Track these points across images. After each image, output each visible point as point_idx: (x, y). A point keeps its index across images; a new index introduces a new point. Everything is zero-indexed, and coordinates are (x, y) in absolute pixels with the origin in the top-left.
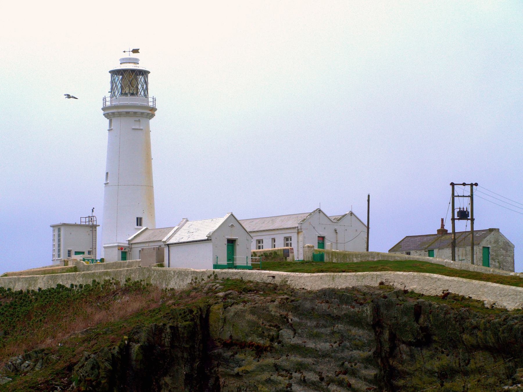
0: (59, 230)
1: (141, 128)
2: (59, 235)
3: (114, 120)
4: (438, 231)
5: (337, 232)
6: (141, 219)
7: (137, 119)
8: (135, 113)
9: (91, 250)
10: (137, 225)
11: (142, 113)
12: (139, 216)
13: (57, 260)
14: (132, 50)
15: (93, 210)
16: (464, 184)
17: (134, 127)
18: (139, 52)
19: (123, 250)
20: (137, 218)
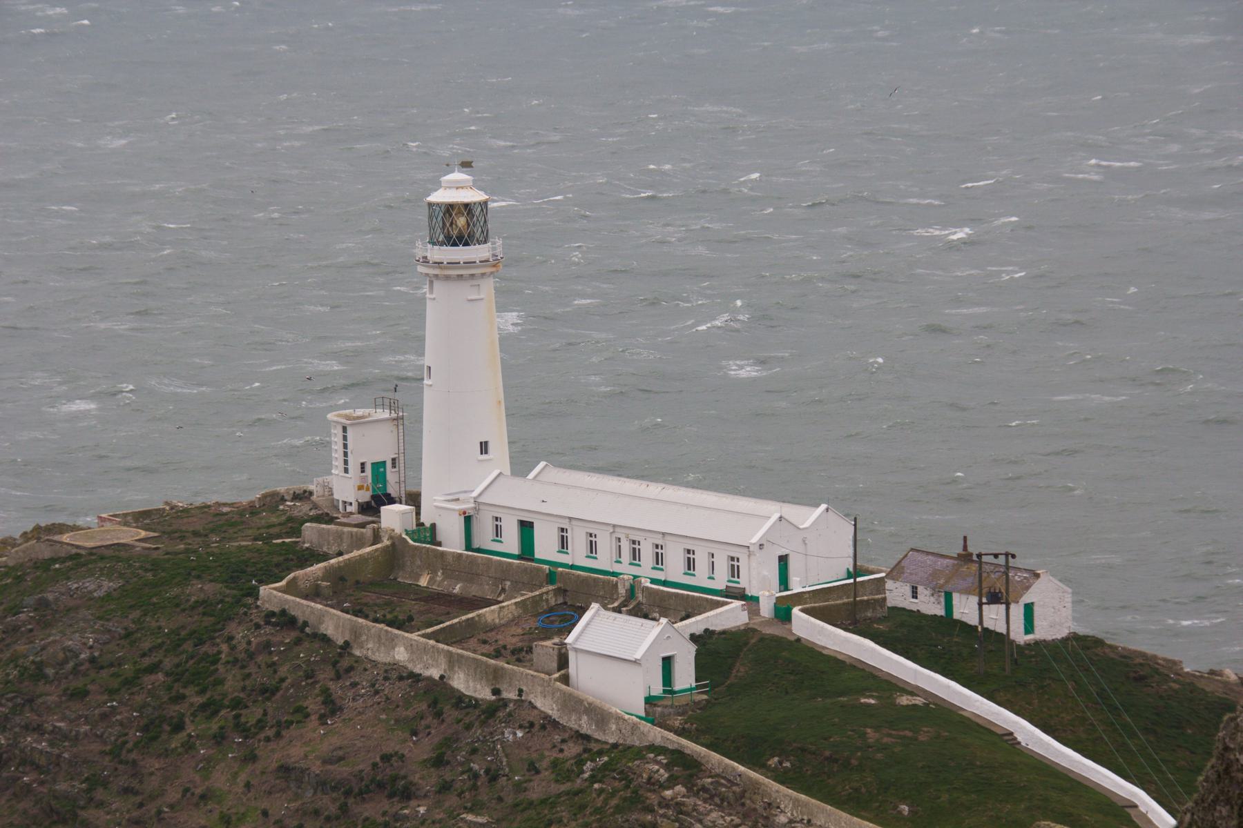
0: (345, 429)
1: (482, 296)
2: (345, 438)
3: (437, 284)
4: (959, 555)
5: (806, 544)
6: (486, 443)
7: (475, 282)
8: (472, 276)
9: (397, 456)
10: (482, 453)
11: (483, 274)
12: (483, 441)
13: (342, 476)
14: (460, 163)
15: (395, 389)
16: (996, 556)
17: (470, 298)
18: (472, 167)
19: (467, 515)
20: (481, 443)
